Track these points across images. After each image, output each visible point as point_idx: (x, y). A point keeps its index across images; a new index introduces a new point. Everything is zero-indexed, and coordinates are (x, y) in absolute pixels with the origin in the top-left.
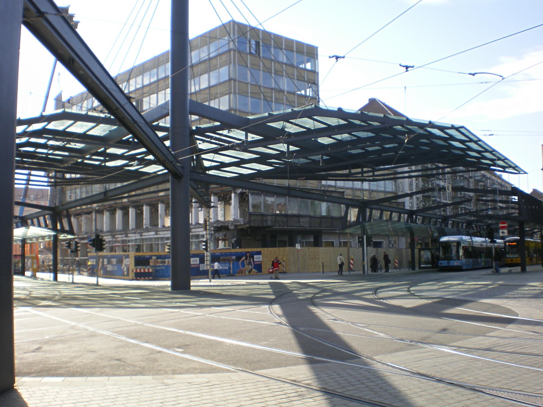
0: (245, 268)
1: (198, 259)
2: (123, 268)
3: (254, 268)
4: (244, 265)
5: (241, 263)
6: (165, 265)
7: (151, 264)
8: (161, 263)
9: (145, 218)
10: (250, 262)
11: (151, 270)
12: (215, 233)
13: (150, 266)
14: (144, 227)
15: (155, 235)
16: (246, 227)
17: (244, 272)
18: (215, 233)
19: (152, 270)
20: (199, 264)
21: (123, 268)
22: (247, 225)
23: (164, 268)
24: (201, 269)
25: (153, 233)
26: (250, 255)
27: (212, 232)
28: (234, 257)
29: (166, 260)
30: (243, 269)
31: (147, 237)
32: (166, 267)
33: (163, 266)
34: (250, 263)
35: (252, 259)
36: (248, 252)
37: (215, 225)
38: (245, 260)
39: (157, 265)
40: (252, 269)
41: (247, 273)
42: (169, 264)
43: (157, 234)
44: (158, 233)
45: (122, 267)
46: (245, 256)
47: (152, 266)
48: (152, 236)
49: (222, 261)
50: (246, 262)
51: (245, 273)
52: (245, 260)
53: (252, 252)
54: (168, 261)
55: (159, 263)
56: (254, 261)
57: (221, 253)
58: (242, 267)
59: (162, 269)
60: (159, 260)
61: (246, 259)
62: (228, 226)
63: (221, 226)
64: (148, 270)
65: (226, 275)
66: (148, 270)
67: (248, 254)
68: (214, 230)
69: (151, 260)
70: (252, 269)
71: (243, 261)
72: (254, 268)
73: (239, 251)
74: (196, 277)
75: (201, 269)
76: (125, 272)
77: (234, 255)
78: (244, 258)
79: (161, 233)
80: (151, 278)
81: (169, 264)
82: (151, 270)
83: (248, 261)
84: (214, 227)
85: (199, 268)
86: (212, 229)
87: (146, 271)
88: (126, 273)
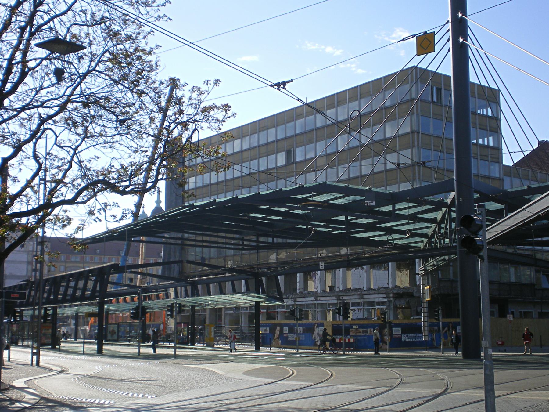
1: (400, 329)
2: (315, 338)
6: (367, 334)
7: (351, 333)
9: (299, 282)
11: (352, 340)
12: (395, 300)
14: (298, 291)
15: (314, 300)
16: (436, 295)
18: (395, 300)
20: (401, 335)
21: (315, 338)
22: (437, 293)
23: (366, 338)
24: (403, 340)
25: (312, 299)
27: (392, 299)
29: (369, 330)
31: (304, 303)
32: (368, 336)
33: (365, 336)
36: (451, 323)
37: (395, 291)
39: (359, 334)
43: (316, 300)
44: (318, 298)
45: (313, 337)
47: (353, 336)
48: (309, 302)
51: (448, 345)
53: (454, 322)
54: (371, 331)
55: (360, 332)
59: (364, 339)
60: (361, 330)
61: (449, 330)
62: (413, 293)
63: (403, 293)
64: (349, 340)
66: (349, 340)
67: (450, 325)
68: (393, 297)
69: (351, 329)
74: (399, 348)
75: (403, 340)
76: (318, 341)
78: (446, 329)
79: (322, 298)
80: (352, 348)
82: (352, 340)
83: (450, 332)
84: (393, 294)
85: (401, 338)
86: (391, 295)
87: (347, 340)
88: (318, 343)
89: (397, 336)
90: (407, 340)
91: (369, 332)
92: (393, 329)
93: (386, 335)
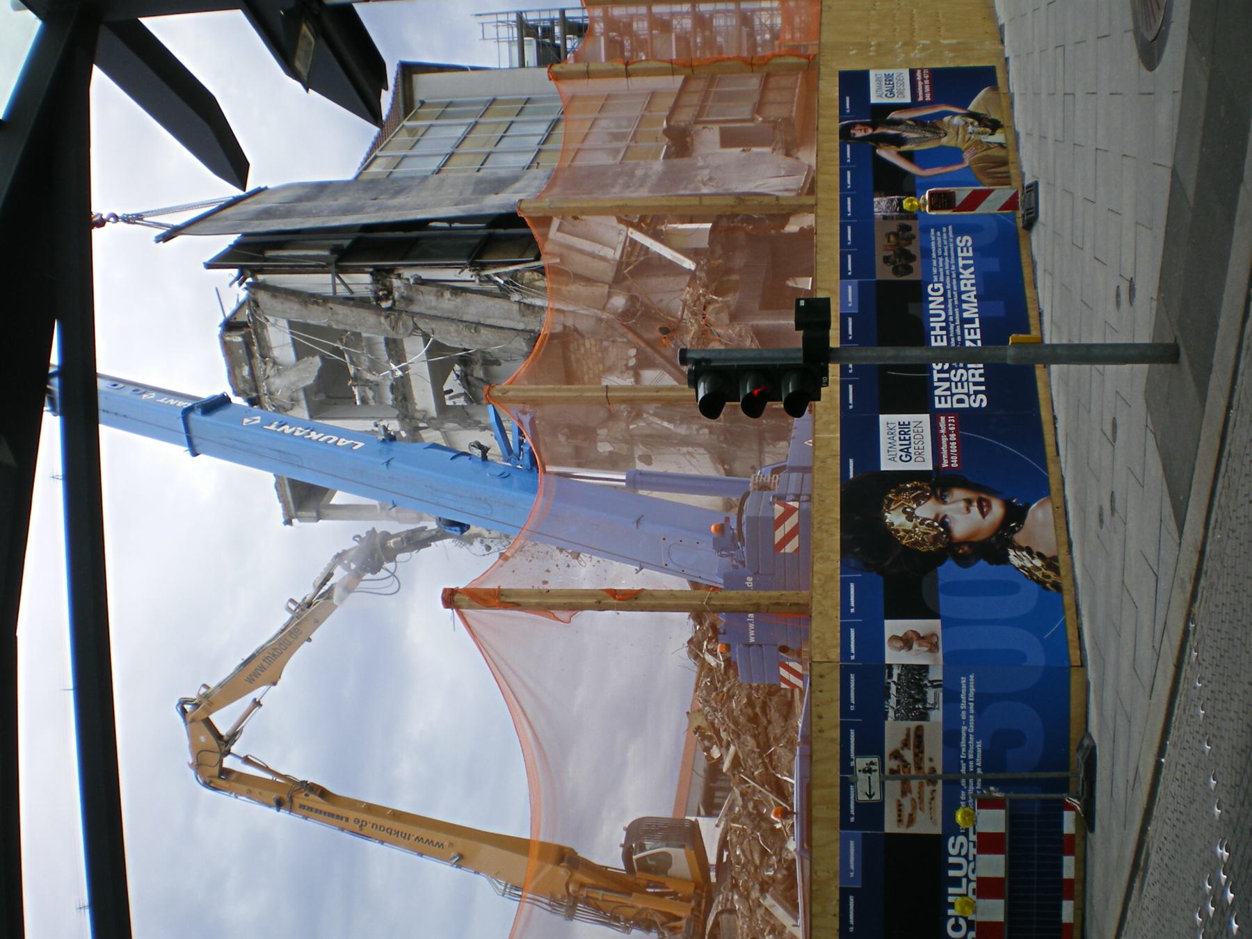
0: (960, 145)
3: (965, 106)
5: (923, 167)
6: (936, 674)
7: (928, 824)
8: (924, 716)
10: (920, 123)
13: (951, 828)
17: (1000, 153)
19: (986, 803)
20: (935, 415)
23: (968, 687)
24: (981, 401)
28: (881, 205)
29: (894, 656)
30: (967, 157)
32: (953, 662)
33: (952, 697)
34: (930, 125)
35: (894, 115)
40: (972, 115)
41: (999, 137)
42: (928, 641)
46: (874, 149)
49: (909, 270)
50: (919, 141)
51: (1001, 145)
54: (906, 642)
57: (844, 274)
59: (982, 701)
60: (894, 731)
61: (897, 141)
64: (987, 843)
67: (859, 133)
71: (909, 156)
75: (981, 401)
78: (888, 154)
80: (1069, 823)
81: (928, 641)
82: (994, 821)
85: (965, 418)
87: (994, 865)
89: (950, 445)
91: (916, 657)
92: (886, 466)
93: (943, 522)
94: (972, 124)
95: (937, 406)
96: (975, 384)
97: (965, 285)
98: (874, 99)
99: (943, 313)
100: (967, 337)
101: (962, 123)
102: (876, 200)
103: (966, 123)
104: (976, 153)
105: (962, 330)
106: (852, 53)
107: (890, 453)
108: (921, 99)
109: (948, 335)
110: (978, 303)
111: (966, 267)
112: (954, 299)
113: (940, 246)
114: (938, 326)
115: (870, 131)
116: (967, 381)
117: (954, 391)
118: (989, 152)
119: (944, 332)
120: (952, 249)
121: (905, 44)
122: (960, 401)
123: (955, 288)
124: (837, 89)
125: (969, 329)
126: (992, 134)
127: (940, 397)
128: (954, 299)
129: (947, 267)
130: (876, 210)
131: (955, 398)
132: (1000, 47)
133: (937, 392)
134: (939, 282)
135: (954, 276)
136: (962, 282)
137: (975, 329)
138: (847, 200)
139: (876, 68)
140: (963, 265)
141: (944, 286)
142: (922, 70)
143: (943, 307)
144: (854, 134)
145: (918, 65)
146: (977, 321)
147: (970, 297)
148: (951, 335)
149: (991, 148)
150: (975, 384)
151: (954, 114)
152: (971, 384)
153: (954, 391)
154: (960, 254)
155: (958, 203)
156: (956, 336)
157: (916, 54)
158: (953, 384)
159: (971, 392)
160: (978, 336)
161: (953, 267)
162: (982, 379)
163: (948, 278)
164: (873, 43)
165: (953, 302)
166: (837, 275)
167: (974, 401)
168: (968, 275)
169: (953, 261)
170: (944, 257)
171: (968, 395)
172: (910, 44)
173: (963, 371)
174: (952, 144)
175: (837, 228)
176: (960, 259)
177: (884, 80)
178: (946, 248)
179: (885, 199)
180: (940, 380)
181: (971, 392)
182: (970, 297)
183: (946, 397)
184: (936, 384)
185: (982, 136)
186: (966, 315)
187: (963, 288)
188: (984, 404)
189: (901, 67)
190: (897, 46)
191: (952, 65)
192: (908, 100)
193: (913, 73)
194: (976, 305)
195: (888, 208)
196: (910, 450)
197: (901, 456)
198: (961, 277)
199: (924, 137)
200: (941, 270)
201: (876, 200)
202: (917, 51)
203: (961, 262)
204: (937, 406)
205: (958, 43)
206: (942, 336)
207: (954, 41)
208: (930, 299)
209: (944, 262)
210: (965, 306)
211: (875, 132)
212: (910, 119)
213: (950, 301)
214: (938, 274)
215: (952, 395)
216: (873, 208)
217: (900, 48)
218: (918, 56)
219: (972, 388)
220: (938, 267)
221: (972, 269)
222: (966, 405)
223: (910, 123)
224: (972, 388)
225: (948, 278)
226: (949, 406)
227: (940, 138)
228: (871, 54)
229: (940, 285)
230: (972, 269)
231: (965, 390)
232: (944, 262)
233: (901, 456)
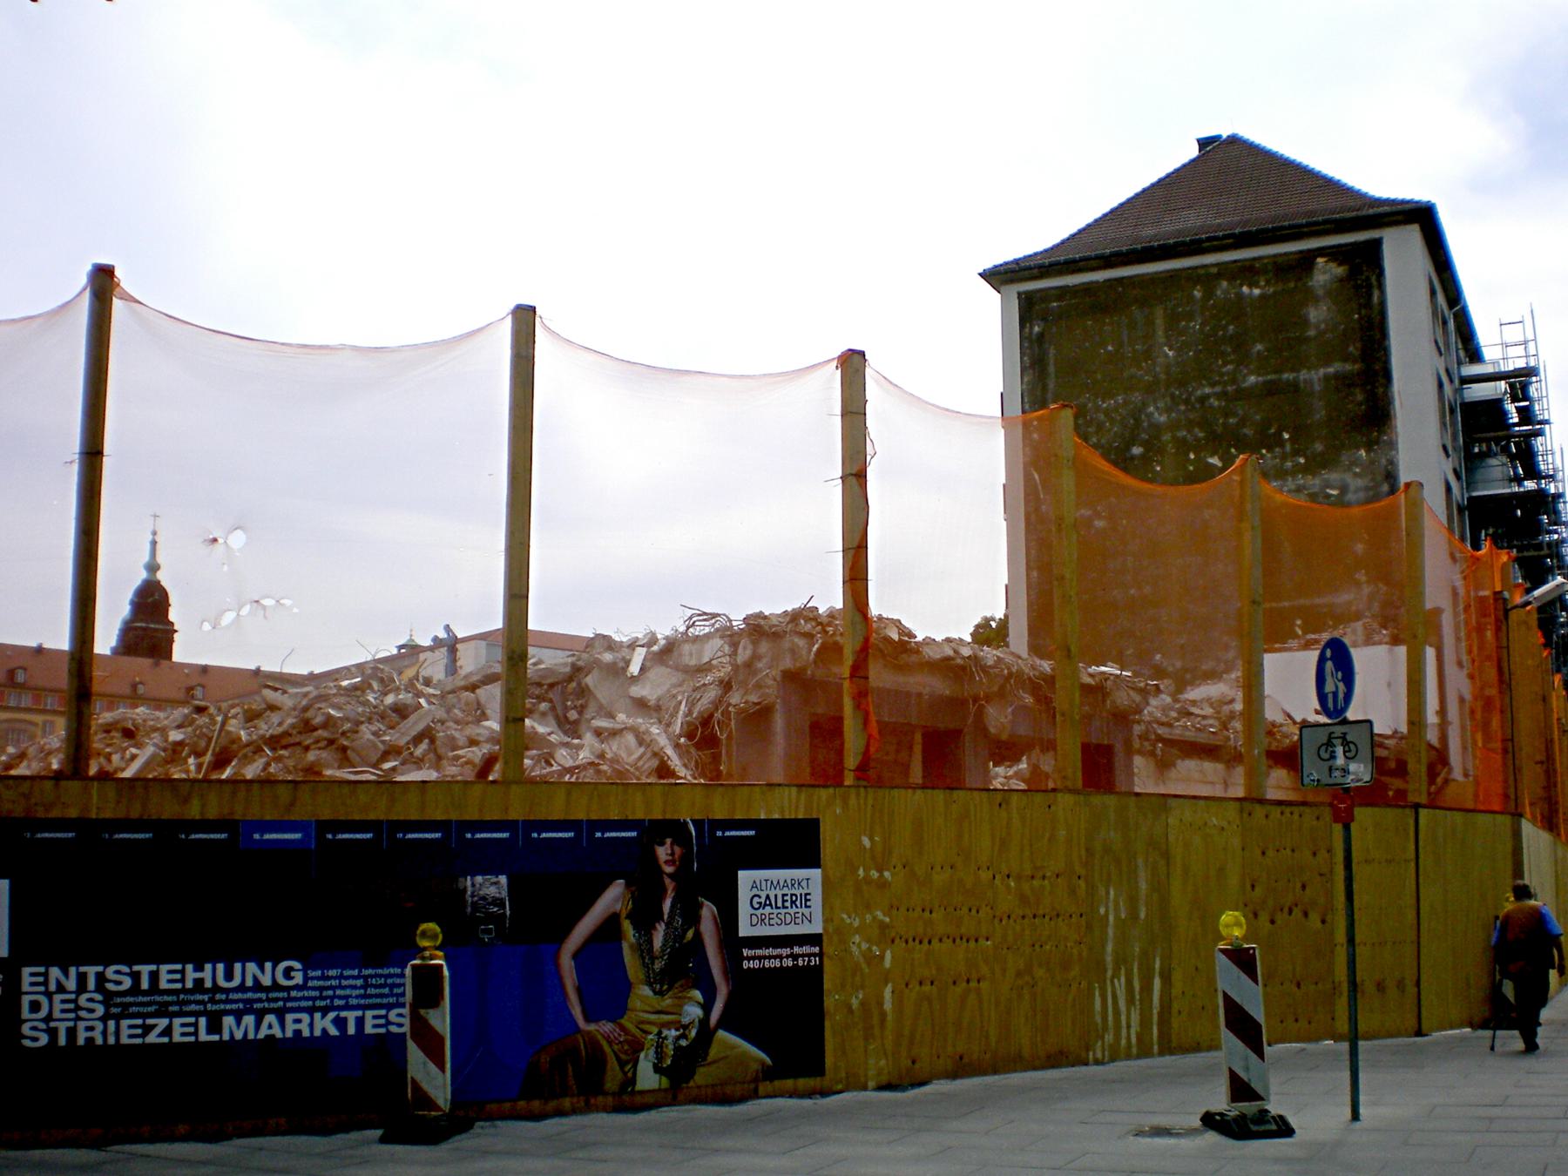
3: (726, 1023)
4: (624, 988)
26: (686, 860)
30: (607, 1027)
35: (708, 911)
38: (628, 927)
41: (647, 1078)
50: (644, 950)
52: (628, 927)
53: (708, 826)
56: (732, 943)
57: (326, 826)
58: (588, 1019)
61: (645, 916)
65: (379, 1132)
67: (662, 853)
70: (706, 1033)
72: (724, 1023)
73: (557, 815)
77: (488, 859)
78: (613, 898)
90: (93, 1029)
94: (684, 1036)
95: (26, 971)
96: (72, 1033)
97: (298, 1021)
98: (746, 878)
99: (236, 982)
100: (177, 1021)
101: (685, 1020)
102: (503, 879)
103: (685, 1027)
104: (610, 1043)
105: (197, 1014)
106: (866, 842)
107: (764, 883)
108: (745, 952)
109: (184, 991)
110: (255, 1040)
111: (340, 1023)
112: (275, 1001)
113: (390, 981)
114: (207, 974)
115: (669, 869)
116: (79, 1018)
117: (58, 998)
118: (612, 1063)
119: (189, 985)
120: (385, 1001)
121: (883, 927)
122: (35, 1007)
123: (289, 1005)
124: (776, 816)
125: (196, 1025)
126: (657, 1069)
127: (46, 975)
128: (275, 1001)
129: (339, 992)
130: (479, 879)
131: (44, 1000)
132: (871, 1084)
133: (55, 972)
134: (306, 978)
135: (319, 1003)
136: (305, 1017)
137: (196, 1034)
138: (752, 830)
139: (826, 883)
140: (345, 1019)
141: (297, 987)
142: (821, 955)
143: (249, 983)
144: (662, 844)
145: (828, 949)
146: (216, 1038)
147: (270, 1027)
148: (182, 996)
149: (622, 1064)
150: (72, 1033)
151: (707, 1007)
152: (71, 1024)
153: (58, 998)
154: (369, 1014)
155: (422, 1012)
156: (190, 1002)
157: (858, 945)
158: (73, 996)
159: (52, 1024)
160: (177, 1038)
161: (337, 1002)
162: (81, 1041)
163: (316, 993)
164: (887, 874)
165: (260, 1000)
166: (326, 814)
167: (34, 1028)
168: (324, 1024)
169: (353, 1002)
170: (365, 987)
171: (49, 1018)
172: (885, 935)
173: (100, 1010)
174: (634, 1002)
175: (439, 816)
176: (359, 1013)
177: (794, 892)
178: (386, 991)
179: (504, 894)
180: (82, 978)
181: (52, 1024)
182: (270, 1027)
183: (46, 983)
184: (73, 970)
185: (652, 1052)
186: (228, 1021)
187: (289, 1017)
188: (27, 1043)
189: (826, 921)
190: (880, 915)
191: (829, 1002)
192: (744, 930)
193: (814, 939)
194: (251, 1036)
195: (484, 898)
196: (768, 908)
197: (760, 897)
198: (318, 1015)
199: (653, 958)
200: (334, 983)
201: (503, 879)
202: (864, 946)
203: (351, 1016)
204: (26, 971)
205: (883, 1015)
206: (182, 980)
207: (888, 1006)
208: (268, 965)
209: (354, 987)
210: (249, 1020)
211: (667, 881)
212: (698, 935)
213: (263, 996)
214: (324, 978)
215: (49, 995)
216: (483, 874)
217: (875, 918)
218: (854, 949)
219: (62, 1027)
220: (341, 977)
221: (333, 1031)
222: (26, 1013)
223: (690, 934)
224: (62, 1027)
225: (316, 993)
226: (25, 987)
227: (650, 984)
228: (861, 872)
229: (298, 978)
230: (333, 1031)
231: (57, 1014)
232: (354, 987)
233: (760, 897)
